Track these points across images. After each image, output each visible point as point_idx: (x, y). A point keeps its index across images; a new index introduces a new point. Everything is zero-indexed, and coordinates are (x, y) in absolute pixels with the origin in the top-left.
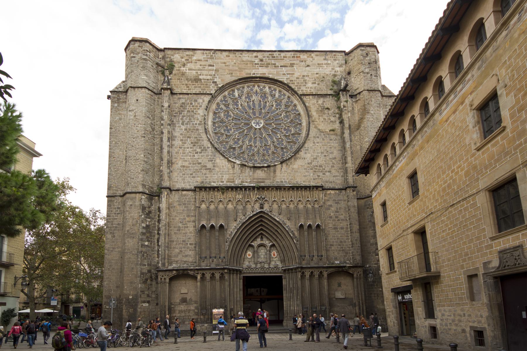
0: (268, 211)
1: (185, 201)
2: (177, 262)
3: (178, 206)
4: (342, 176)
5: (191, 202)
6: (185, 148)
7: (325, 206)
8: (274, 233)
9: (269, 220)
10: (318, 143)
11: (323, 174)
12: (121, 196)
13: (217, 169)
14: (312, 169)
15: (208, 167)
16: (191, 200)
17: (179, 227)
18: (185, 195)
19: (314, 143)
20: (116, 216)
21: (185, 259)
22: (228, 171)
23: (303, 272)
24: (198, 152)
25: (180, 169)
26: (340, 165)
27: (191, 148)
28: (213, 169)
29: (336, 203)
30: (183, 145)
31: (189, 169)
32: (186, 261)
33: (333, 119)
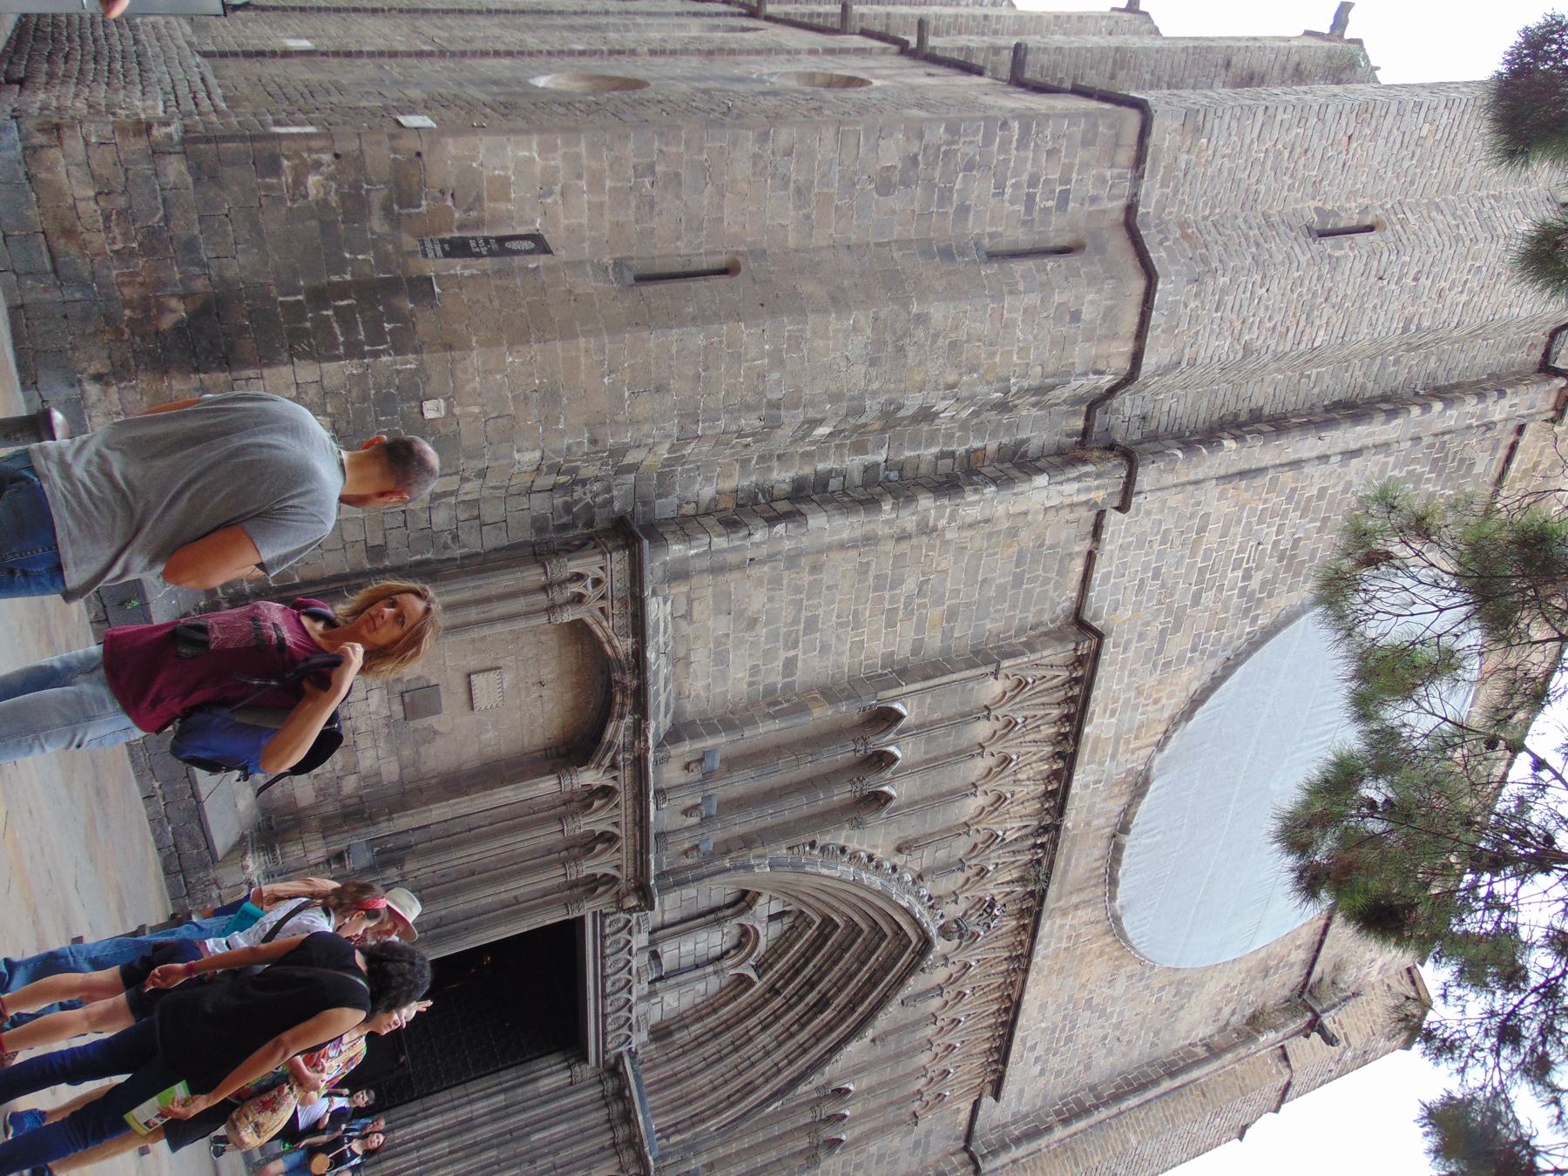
2: (688, 616)
3: (1015, 549)
4: (1014, 1115)
5: (1025, 609)
8: (811, 984)
9: (885, 968)
10: (1159, 999)
11: (1037, 1059)
12: (1131, 209)
14: (1064, 1018)
16: (1032, 609)
17: (897, 583)
18: (1062, 572)
19: (1162, 989)
20: (1016, 186)
21: (700, 656)
25: (1192, 516)
26: (1059, 1092)
29: (917, 1144)
31: (1182, 557)
33: (1226, 1011)
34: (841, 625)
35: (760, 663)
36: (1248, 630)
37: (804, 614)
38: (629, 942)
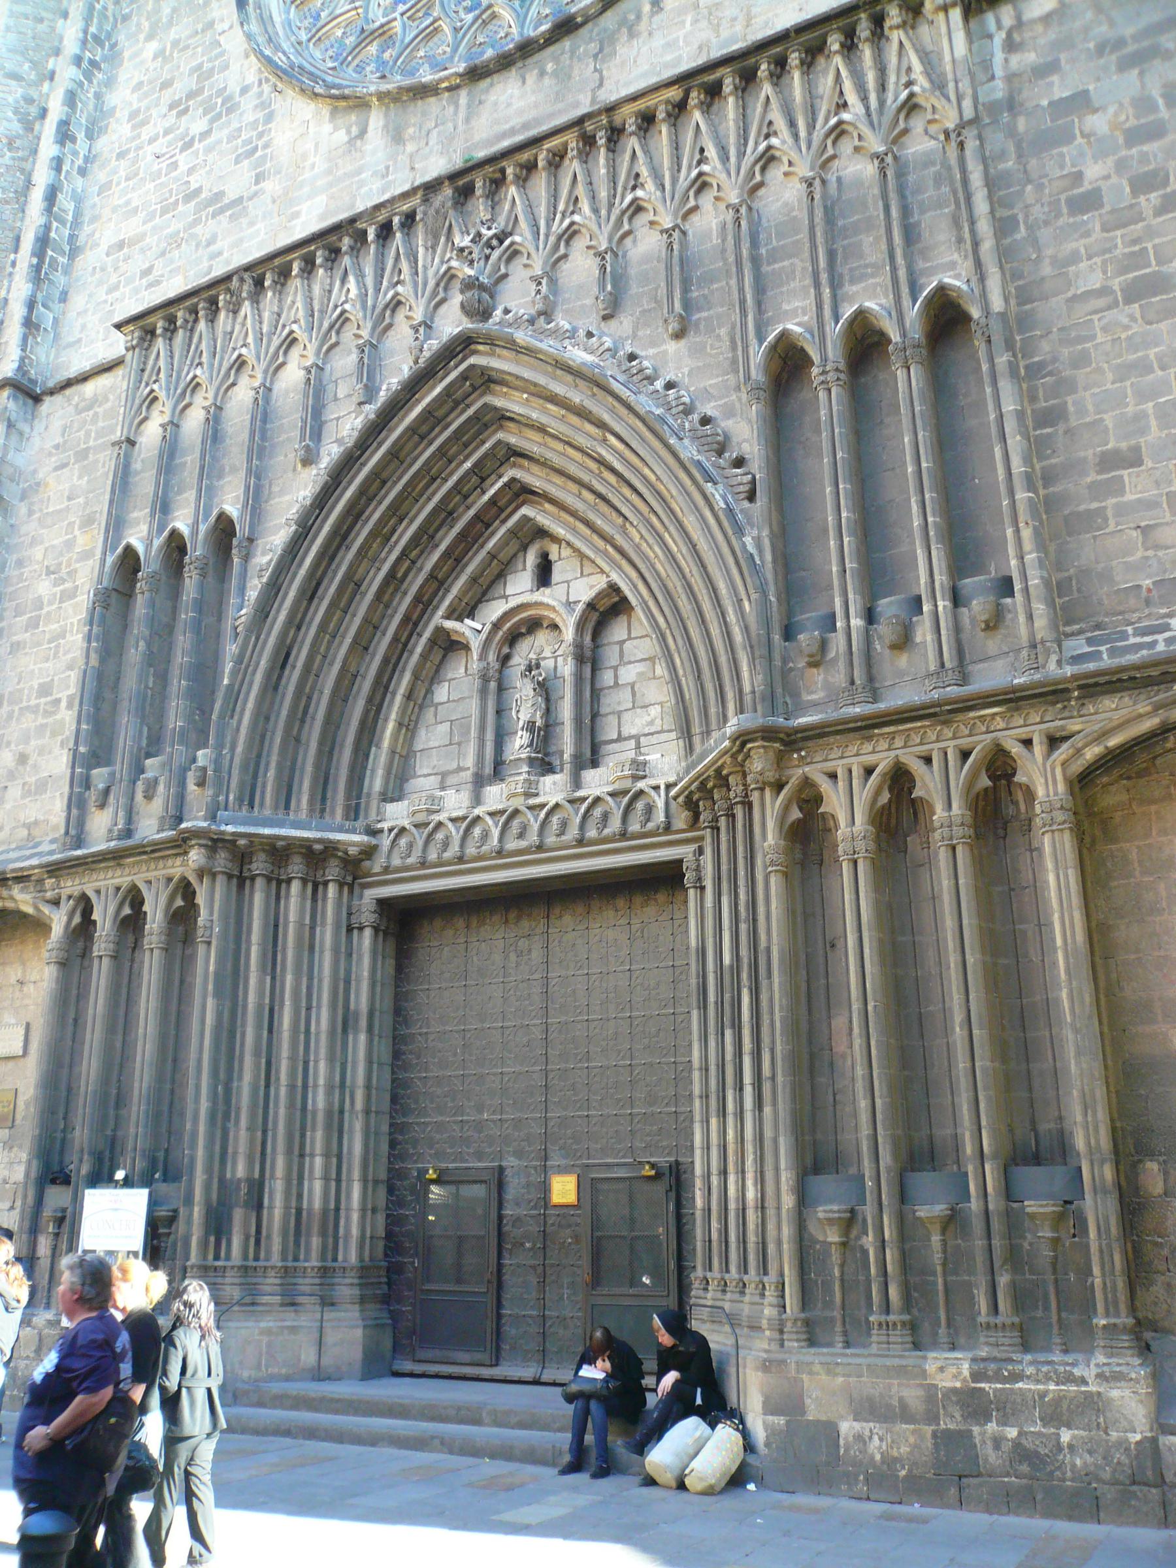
0: (517, 323)
1: (88, 434)
6: (139, 148)
7: (1021, 124)
13: (270, 186)
15: (231, 195)
17: (39, 604)
18: (94, 402)
22: (329, 172)
23: (807, 783)
24: (193, 139)
27: (167, 132)
28: (256, 194)
30: (134, 139)
32: (36, 823)
34: (55, 656)
35: (60, 738)
36: (255, 89)
37: (33, 702)
38: (440, 824)
